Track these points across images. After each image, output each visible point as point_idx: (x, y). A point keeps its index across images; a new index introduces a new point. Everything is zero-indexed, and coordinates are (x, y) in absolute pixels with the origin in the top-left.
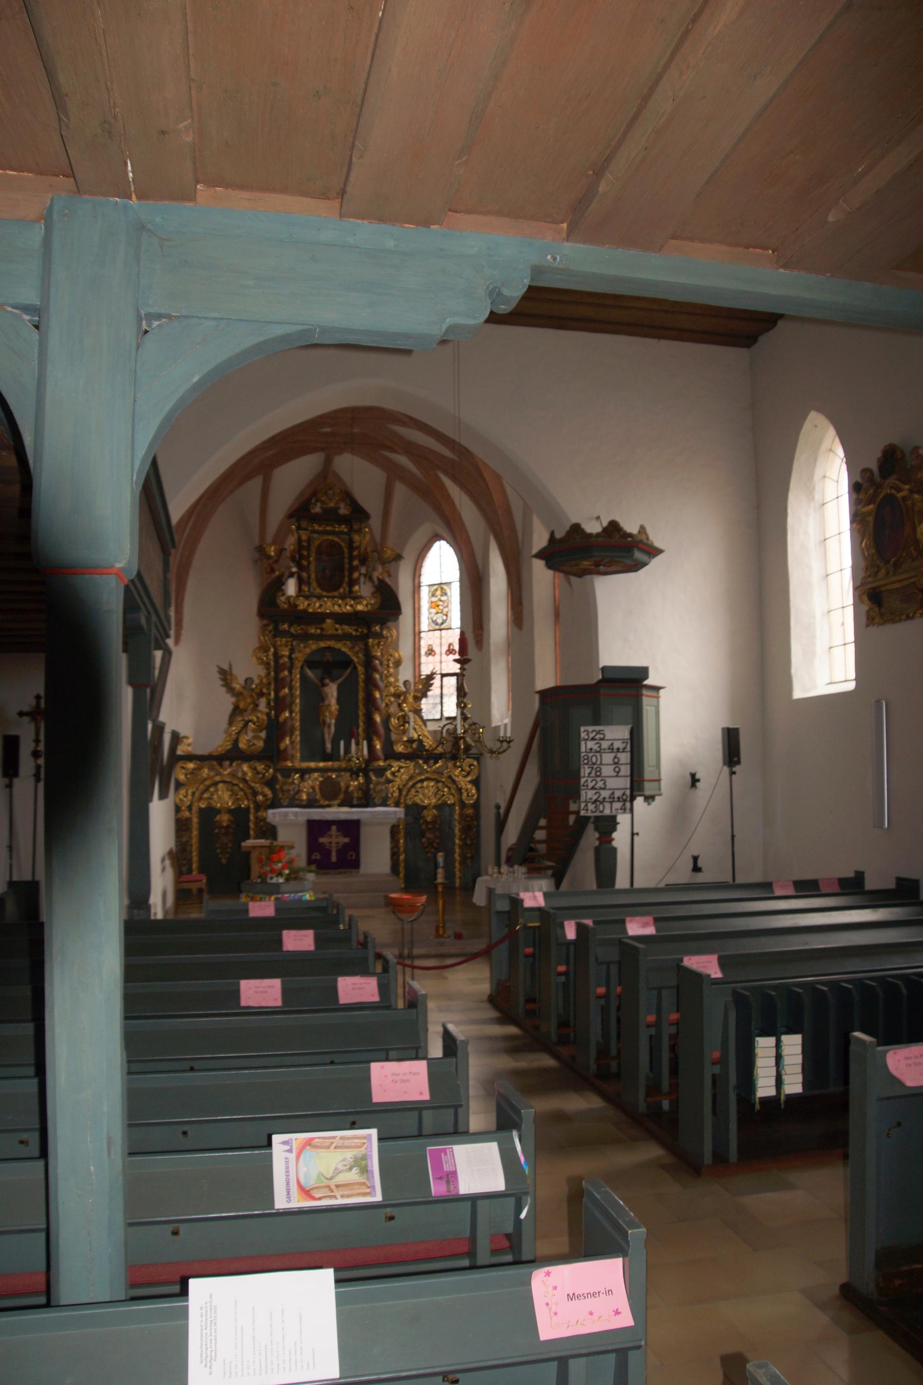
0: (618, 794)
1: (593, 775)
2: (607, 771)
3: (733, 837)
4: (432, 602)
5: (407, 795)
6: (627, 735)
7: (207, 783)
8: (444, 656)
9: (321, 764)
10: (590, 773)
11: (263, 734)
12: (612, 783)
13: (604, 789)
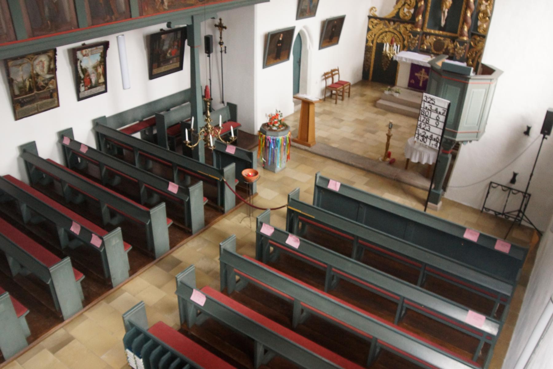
0: (435, 136)
1: (425, 121)
2: (432, 122)
3: (532, 175)
6: (446, 107)
7: (381, 31)
9: (437, 32)
10: (423, 120)
11: (412, 11)
12: (433, 129)
13: (429, 131)
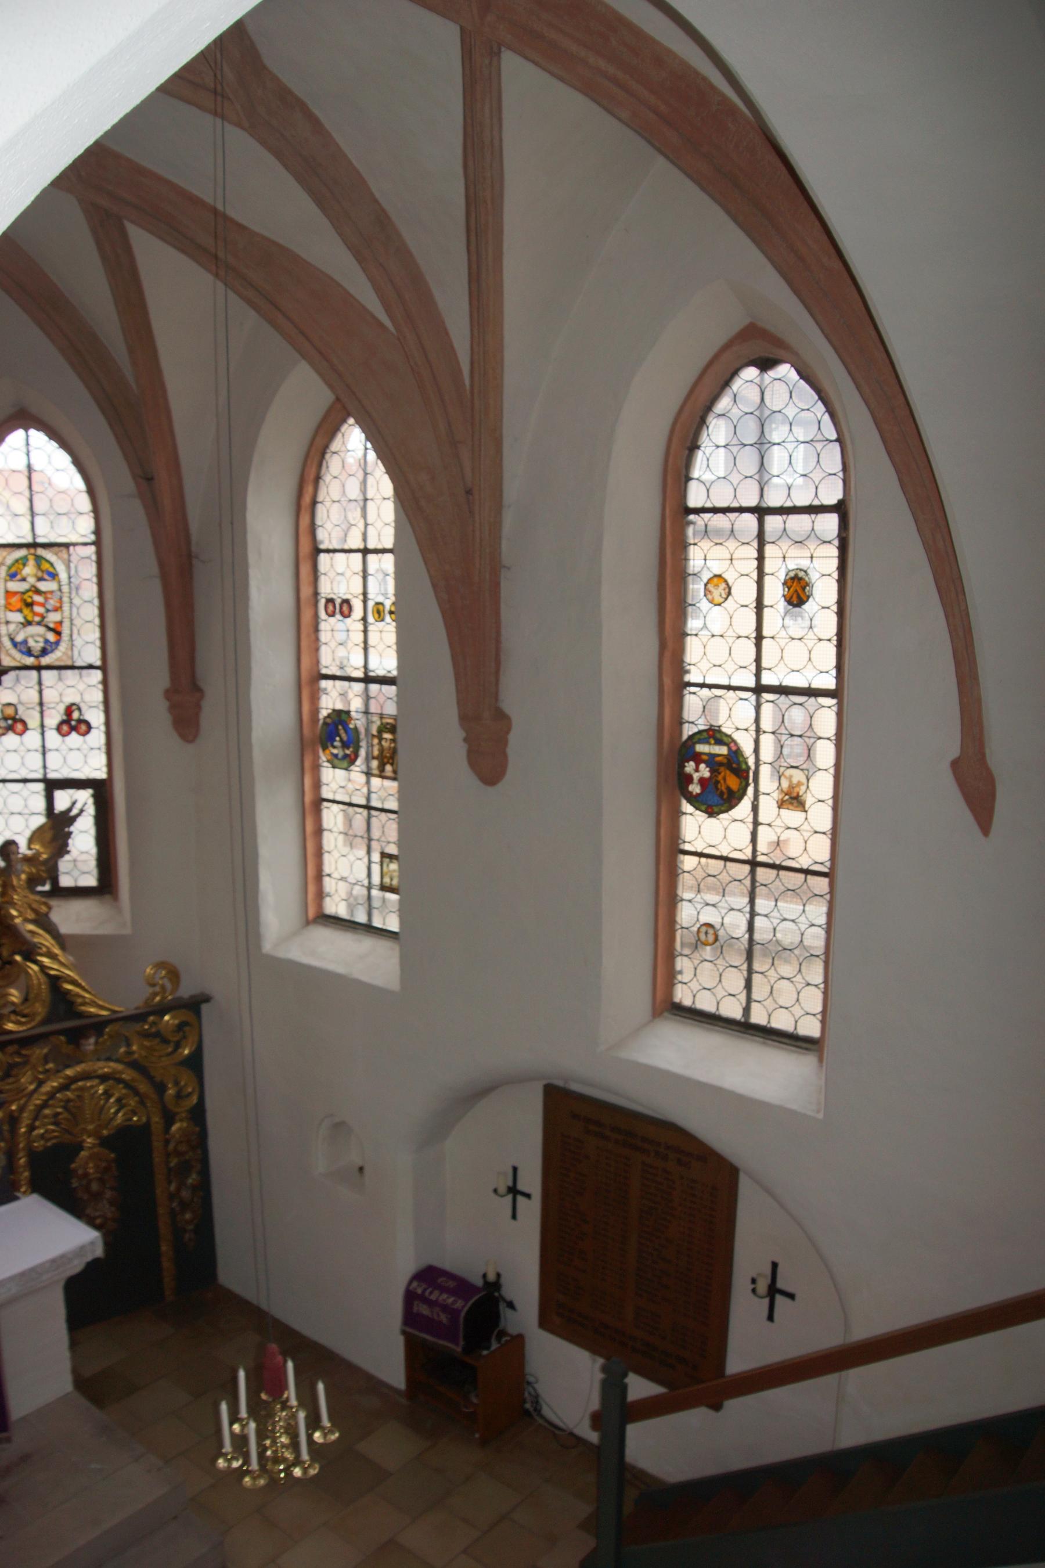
4: (9, 594)
5: (32, 1128)
8: (53, 738)
